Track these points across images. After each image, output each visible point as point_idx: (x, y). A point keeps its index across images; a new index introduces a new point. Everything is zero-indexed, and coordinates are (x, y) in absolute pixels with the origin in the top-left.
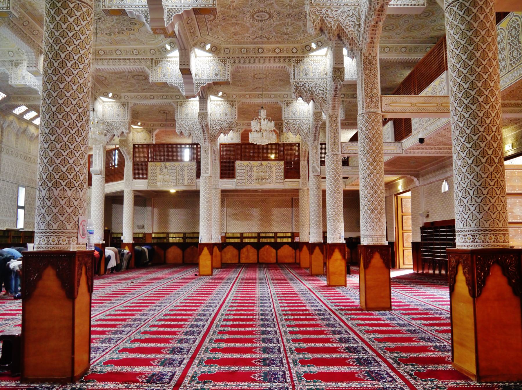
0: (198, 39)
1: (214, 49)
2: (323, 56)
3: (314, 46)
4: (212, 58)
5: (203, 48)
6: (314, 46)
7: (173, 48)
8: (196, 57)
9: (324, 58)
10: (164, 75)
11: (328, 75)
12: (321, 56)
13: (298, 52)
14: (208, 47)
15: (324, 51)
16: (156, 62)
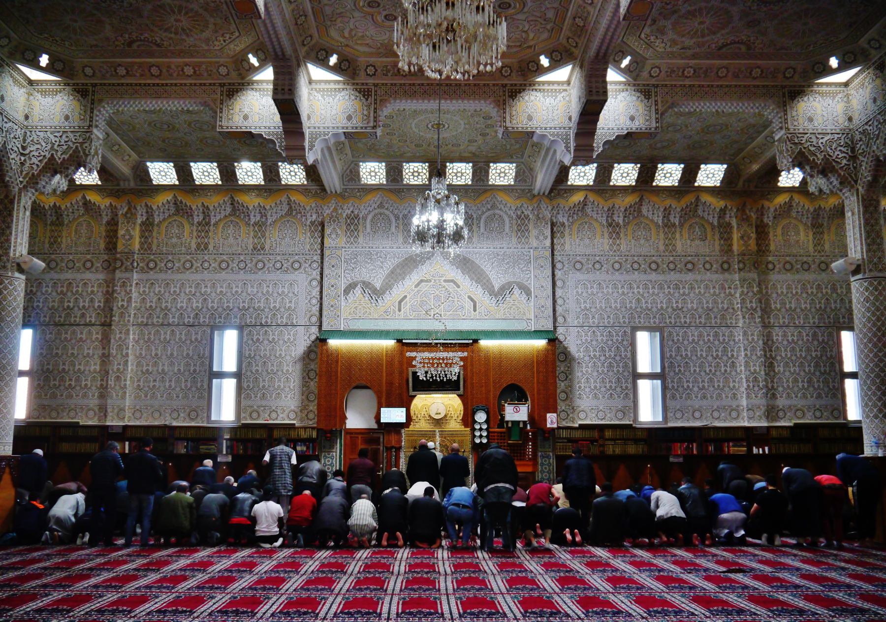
0: (314, 42)
1: (344, 65)
2: (562, 83)
3: (544, 61)
4: (341, 86)
5: (322, 62)
6: (544, 61)
7: (263, 63)
8: (310, 83)
9: (565, 87)
10: (246, 117)
11: (573, 119)
12: (558, 83)
13: (513, 74)
14: (333, 60)
15: (563, 73)
16: (229, 91)
